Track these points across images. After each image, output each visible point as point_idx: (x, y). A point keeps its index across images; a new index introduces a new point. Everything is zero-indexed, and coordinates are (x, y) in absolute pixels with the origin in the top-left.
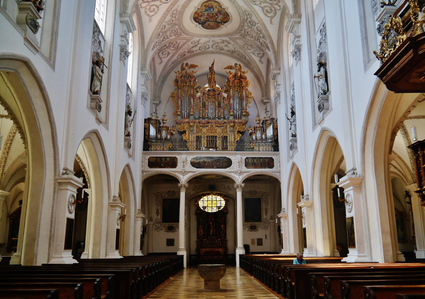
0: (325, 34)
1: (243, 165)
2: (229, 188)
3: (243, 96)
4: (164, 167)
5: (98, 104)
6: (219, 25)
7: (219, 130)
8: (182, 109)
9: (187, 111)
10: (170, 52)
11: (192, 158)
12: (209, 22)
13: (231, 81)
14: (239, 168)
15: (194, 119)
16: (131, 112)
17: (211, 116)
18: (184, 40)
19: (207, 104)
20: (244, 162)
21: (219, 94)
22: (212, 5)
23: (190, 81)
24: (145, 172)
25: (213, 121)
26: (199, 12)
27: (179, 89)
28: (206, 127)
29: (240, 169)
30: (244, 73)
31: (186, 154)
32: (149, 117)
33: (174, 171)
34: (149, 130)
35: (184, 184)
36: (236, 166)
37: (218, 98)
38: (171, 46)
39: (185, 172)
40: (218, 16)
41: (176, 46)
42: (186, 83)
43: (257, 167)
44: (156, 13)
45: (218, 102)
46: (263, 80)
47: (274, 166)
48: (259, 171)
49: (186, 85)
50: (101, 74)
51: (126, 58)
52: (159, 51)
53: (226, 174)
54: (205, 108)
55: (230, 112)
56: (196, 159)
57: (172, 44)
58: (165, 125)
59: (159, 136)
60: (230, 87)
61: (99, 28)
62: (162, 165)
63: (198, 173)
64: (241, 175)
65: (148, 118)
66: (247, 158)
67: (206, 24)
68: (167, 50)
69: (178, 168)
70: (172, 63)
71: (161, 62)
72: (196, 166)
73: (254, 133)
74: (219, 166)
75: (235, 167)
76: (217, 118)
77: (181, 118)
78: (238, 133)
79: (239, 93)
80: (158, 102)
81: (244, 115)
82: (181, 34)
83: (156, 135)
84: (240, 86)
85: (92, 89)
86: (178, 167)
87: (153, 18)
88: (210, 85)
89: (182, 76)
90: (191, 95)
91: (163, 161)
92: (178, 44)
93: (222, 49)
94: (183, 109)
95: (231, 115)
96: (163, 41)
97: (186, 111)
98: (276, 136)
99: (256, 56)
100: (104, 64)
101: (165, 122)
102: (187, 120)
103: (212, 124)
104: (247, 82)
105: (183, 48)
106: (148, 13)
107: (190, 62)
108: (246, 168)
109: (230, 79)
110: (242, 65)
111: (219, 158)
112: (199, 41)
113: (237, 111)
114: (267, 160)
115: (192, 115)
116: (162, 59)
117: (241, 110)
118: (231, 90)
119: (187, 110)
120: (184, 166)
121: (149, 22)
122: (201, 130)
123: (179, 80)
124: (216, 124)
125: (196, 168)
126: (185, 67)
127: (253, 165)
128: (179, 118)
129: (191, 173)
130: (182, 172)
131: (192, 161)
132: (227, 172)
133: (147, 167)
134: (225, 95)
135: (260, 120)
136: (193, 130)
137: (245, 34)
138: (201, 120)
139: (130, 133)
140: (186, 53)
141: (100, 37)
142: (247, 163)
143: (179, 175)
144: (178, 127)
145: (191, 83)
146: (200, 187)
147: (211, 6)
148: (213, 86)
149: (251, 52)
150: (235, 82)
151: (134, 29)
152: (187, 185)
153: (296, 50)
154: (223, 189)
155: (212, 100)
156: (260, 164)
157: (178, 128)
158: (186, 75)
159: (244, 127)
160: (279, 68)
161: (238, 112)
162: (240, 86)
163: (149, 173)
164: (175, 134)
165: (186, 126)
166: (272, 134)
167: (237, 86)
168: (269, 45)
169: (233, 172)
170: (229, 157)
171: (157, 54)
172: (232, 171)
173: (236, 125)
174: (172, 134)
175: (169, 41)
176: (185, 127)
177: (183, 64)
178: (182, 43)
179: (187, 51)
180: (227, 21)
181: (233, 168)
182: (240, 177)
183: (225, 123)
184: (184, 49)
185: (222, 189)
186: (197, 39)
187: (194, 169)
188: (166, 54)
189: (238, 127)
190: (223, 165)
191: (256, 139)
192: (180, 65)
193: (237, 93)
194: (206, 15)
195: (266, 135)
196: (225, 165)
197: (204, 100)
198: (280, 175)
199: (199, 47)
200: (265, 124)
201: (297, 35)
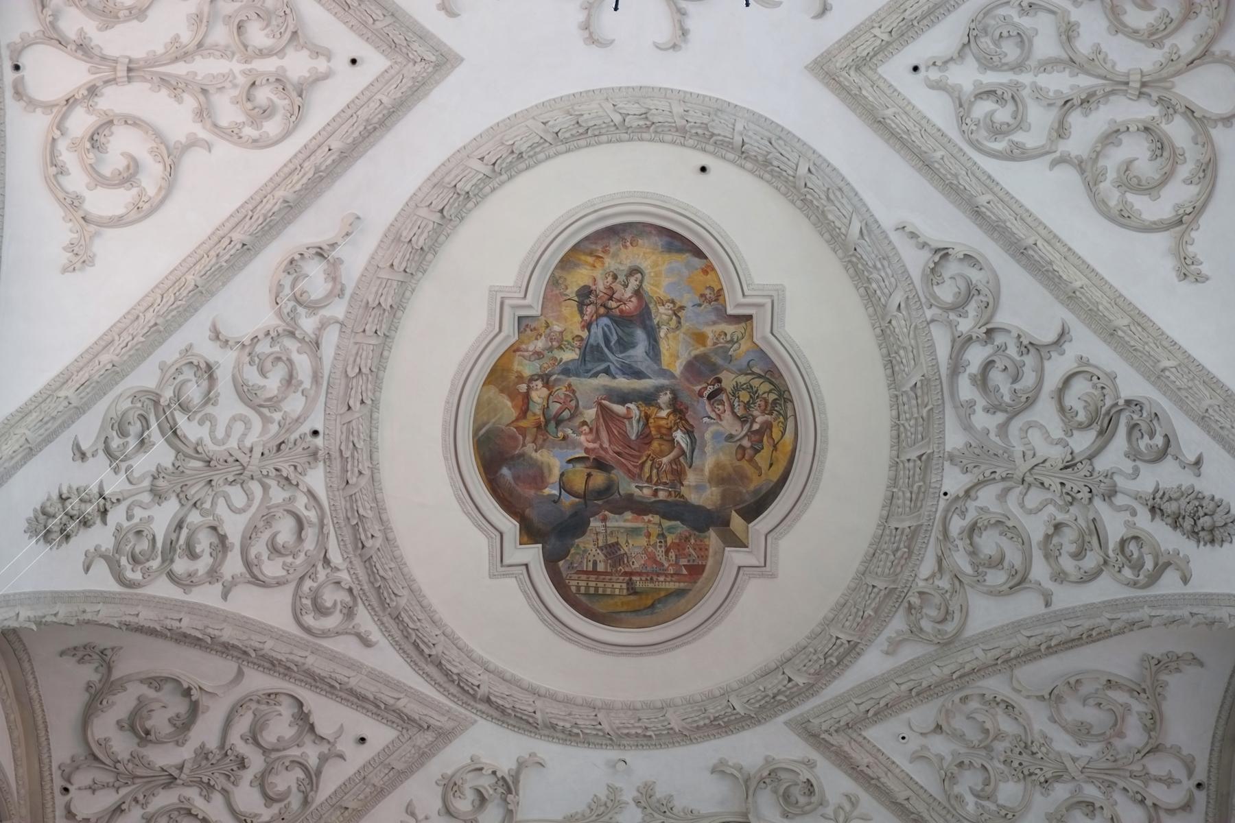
6: (703, 549)
22: (638, 293)
26: (528, 369)
40: (689, 433)
41: (285, 781)
44: (143, 211)
67: (588, 548)
82: (349, 613)
87: (108, 245)
106: (76, 181)
112: (516, 780)
121: (69, 269)
137: (944, 583)
147: (631, 306)
180: (775, 476)
194: (590, 414)
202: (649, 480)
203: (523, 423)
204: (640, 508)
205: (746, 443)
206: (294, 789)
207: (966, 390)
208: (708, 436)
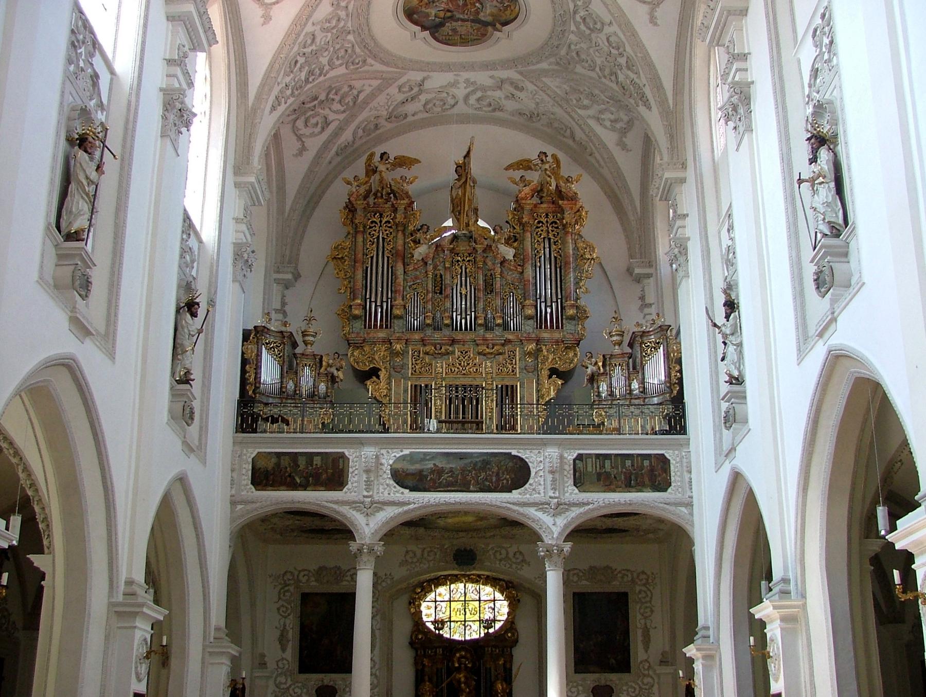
0: (831, 42)
1: (566, 479)
2: (521, 558)
3: (567, 256)
4: (304, 487)
5: (79, 274)
7: (489, 364)
8: (368, 297)
9: (385, 305)
10: (332, 116)
11: (398, 455)
12: (454, 24)
13: (528, 207)
14: (554, 489)
16: (198, 304)
17: (463, 321)
18: (375, 78)
19: (448, 281)
20: (572, 472)
21: (489, 247)
23: (395, 210)
24: (240, 503)
25: (470, 336)
27: (356, 232)
28: (446, 357)
29: (557, 495)
30: (568, 180)
32: (259, 322)
33: (336, 499)
34: (258, 368)
35: (368, 542)
36: (542, 483)
37: (485, 263)
38: (333, 100)
39: (372, 503)
40: (481, 4)
42: (381, 215)
43: (612, 487)
45: (486, 275)
46: (632, 201)
47: (670, 485)
48: (622, 501)
49: (381, 222)
50: (93, 175)
51: (184, 130)
52: (294, 116)
53: (509, 509)
54: (441, 293)
55: (523, 307)
57: (336, 94)
58: (310, 350)
59: (291, 385)
60: (524, 226)
61: (92, 32)
62: (298, 481)
63: (416, 505)
64: (560, 514)
65: (255, 327)
66: (580, 457)
68: (322, 111)
69: (349, 489)
70: (337, 154)
71: (303, 149)
72: (410, 484)
73: (605, 374)
76: (480, 325)
77: (365, 328)
78: (550, 377)
79: (553, 247)
80: (289, 276)
81: (572, 318)
82: (365, 61)
83: (282, 382)
84: (556, 223)
85: (63, 225)
86: (349, 486)
88: (458, 220)
89: (369, 192)
90: (397, 252)
91: (302, 467)
92: (355, 92)
93: (500, 109)
94: (370, 298)
95: (529, 318)
96: (307, 81)
97: (378, 304)
98: (675, 383)
99: (606, 127)
100: (105, 146)
101: (311, 339)
102: (382, 334)
103: (466, 346)
104: (578, 211)
105: (371, 105)
107: (395, 148)
108: (576, 491)
109: (524, 202)
110: (561, 156)
111: (485, 458)
112: (423, 82)
113: (549, 304)
114: (646, 463)
115: (399, 317)
116: (304, 140)
117: (561, 299)
118: (528, 235)
119: (382, 302)
120: (369, 485)
122: (431, 364)
123: (360, 204)
124: (478, 345)
125: (411, 490)
126: (377, 164)
128: (358, 325)
130: (362, 503)
131: (398, 466)
132: (513, 504)
133: (247, 485)
134: (508, 252)
135: (622, 334)
136: (403, 366)
138: (429, 332)
139: (192, 372)
140: (382, 122)
141: (97, 61)
142: (580, 473)
143: (354, 513)
144: (352, 354)
145: (398, 216)
146: (426, 555)
148: (468, 225)
149: (589, 117)
150: (541, 211)
151: (213, 41)
152: (379, 549)
153: (735, 99)
154: (501, 560)
155: (466, 269)
156: (623, 477)
157: (352, 359)
158: (383, 188)
159: (571, 354)
160: (683, 164)
161: (551, 306)
162: (556, 223)
163: (254, 506)
164: (341, 380)
165: (381, 352)
166: (663, 378)
167: (547, 222)
168: (647, 91)
170: (519, 455)
171: (290, 126)
172: (532, 501)
173: (544, 348)
174: (333, 379)
175: (327, 85)
176: (376, 357)
177: (372, 155)
178: (368, 90)
179: (385, 113)
180: (512, 17)
181: (534, 490)
182: (556, 520)
183: (508, 342)
184: (376, 109)
185: (498, 562)
186: (417, 76)
187: (402, 493)
188: (317, 124)
189: (551, 357)
190: (498, 480)
191: (611, 394)
192: (365, 158)
193: (547, 245)
195: (643, 382)
196: (508, 481)
197: (439, 268)
198: (691, 514)
199: (423, 102)
201: (736, 52)
202: (467, 14)
203: (421, 4)
204: (463, 20)
205: (501, 8)
206: (350, 100)
207: (578, 18)
208: (488, 5)
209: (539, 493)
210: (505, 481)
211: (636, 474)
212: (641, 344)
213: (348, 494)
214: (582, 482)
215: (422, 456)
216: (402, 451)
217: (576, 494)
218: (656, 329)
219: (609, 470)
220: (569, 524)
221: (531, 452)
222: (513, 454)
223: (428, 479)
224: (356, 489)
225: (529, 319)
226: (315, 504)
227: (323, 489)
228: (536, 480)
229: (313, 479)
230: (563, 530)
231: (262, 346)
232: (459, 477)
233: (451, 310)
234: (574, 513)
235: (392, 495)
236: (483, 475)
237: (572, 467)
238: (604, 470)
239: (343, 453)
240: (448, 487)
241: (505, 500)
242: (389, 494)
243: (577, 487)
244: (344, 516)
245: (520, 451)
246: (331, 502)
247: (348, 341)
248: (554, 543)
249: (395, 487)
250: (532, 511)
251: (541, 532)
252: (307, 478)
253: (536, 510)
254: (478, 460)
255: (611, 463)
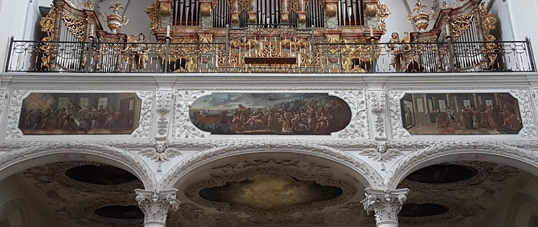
1: (393, 120)
4: (85, 131)
9: (193, 5)
11: (198, 97)
15: (214, 26)
20: (400, 113)
29: (384, 136)
31: (174, 83)
35: (158, 191)
36: (366, 125)
39: (166, 146)
47: (521, 127)
48: (465, 144)
53: (328, 152)
56: (211, 102)
62: (78, 123)
63: (218, 149)
64: (389, 158)
66: (408, 97)
72: (212, 126)
74: (301, 125)
75: (365, 130)
86: (140, 128)
91: (83, 109)
102: (190, 30)
108: (407, 133)
111: (298, 99)
114: (489, 103)
115: (207, 14)
120: (163, 125)
125: (213, 133)
127: (433, 121)
129: (193, 152)
131: (199, 107)
142: (410, 113)
143: (144, 158)
156: (462, 118)
163: (19, 151)
169: (357, 147)
170: (338, 95)
172: (355, 143)
182: (385, 164)
190: (315, 121)
196: (325, 122)
200: (450, 25)
209: (363, 136)
210: (322, 123)
211: (478, 115)
212: (449, 21)
213: (138, 137)
214: (413, 123)
215: (227, 98)
216: (203, 92)
217: (407, 136)
218: (466, 5)
219: (445, 111)
220: (402, 169)
221: (350, 92)
222: (329, 94)
223: (233, 121)
224: (147, 132)
225: (331, 17)
226: (99, 149)
227: (108, 132)
228: (359, 122)
229: (96, 123)
230: (396, 176)
231: (60, 23)
232: (269, 119)
233: (256, 10)
234: (407, 156)
235: (190, 137)
236: (296, 116)
237: (399, 107)
238: (438, 110)
239: (135, 94)
240: (256, 129)
241: (323, 143)
242: (187, 137)
243: (407, 129)
244: (133, 163)
245: (338, 91)
246: (115, 146)
247: (156, 34)
248: (385, 189)
249: (194, 129)
250: (355, 155)
251: (368, 178)
252: (89, 121)
253: (360, 154)
254: (290, 101)
255: (446, 102)
